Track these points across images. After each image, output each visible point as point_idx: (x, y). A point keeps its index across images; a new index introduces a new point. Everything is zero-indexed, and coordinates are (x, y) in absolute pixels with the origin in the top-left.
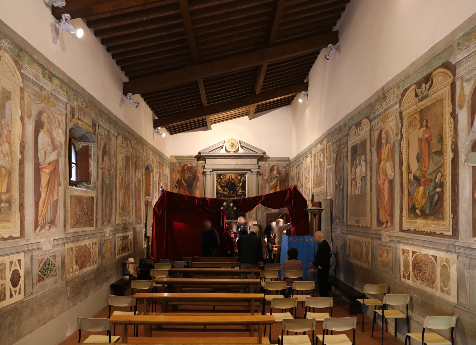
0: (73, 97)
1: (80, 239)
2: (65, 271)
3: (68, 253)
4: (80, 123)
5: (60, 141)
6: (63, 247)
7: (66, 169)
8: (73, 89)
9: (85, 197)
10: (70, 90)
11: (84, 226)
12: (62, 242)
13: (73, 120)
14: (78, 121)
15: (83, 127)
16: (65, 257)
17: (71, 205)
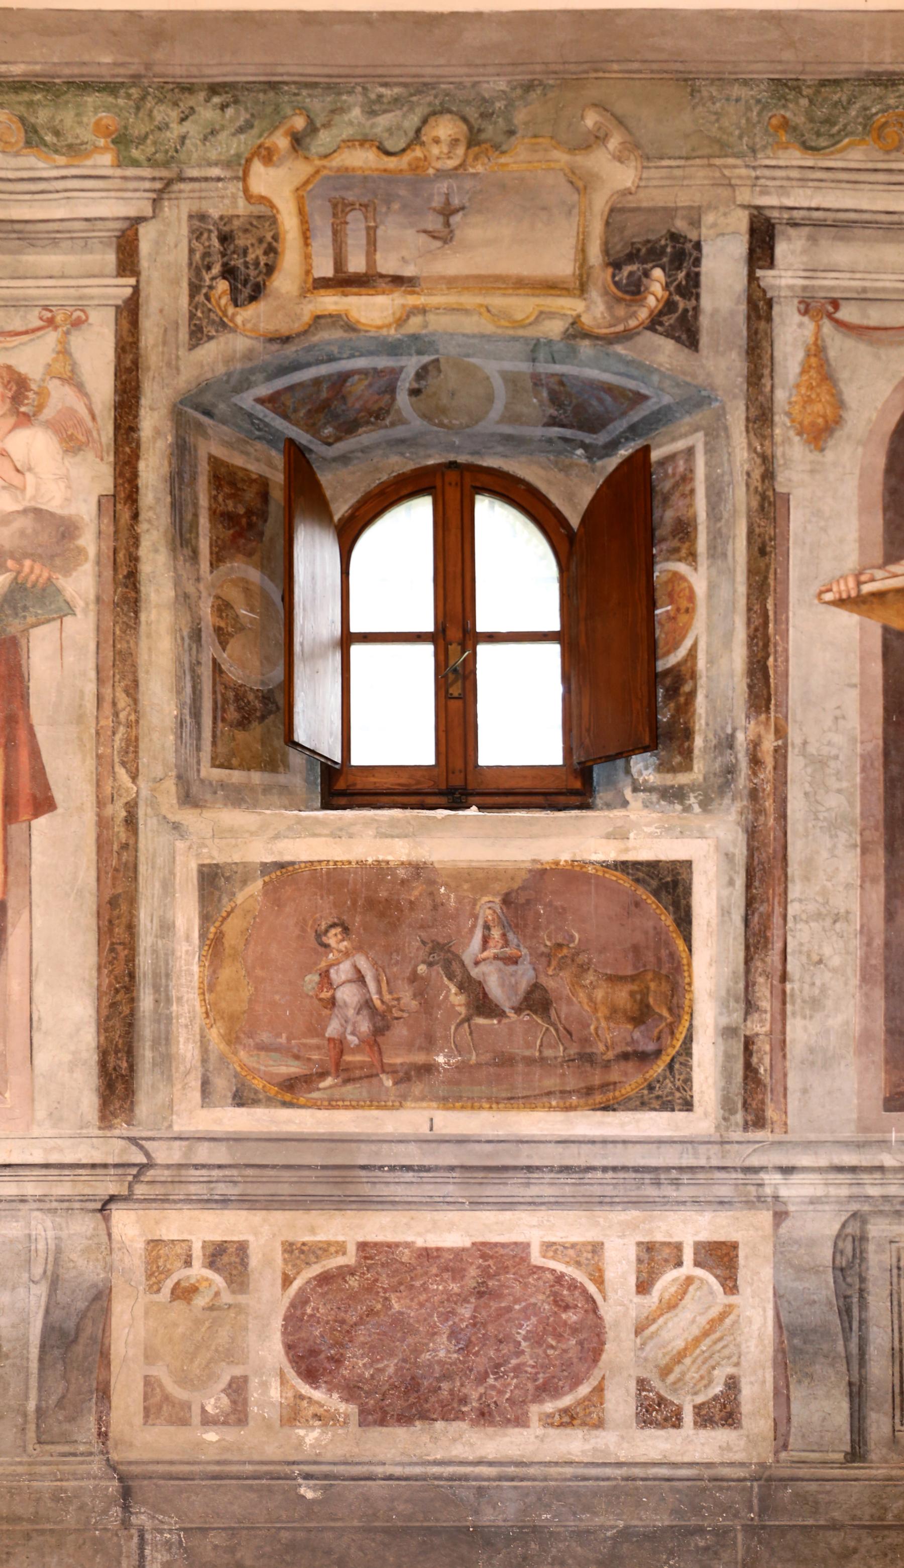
0: (230, 145)
1: (400, 1191)
2: (104, 1393)
3: (155, 1273)
4: (373, 310)
5: (38, 513)
6: (83, 1226)
7: (133, 690)
8: (214, 89)
9: (477, 879)
10: (164, 113)
11: (450, 1100)
12: (65, 1189)
13: (245, 315)
14: (330, 302)
15: (438, 323)
16: (101, 1299)
17: (214, 946)
